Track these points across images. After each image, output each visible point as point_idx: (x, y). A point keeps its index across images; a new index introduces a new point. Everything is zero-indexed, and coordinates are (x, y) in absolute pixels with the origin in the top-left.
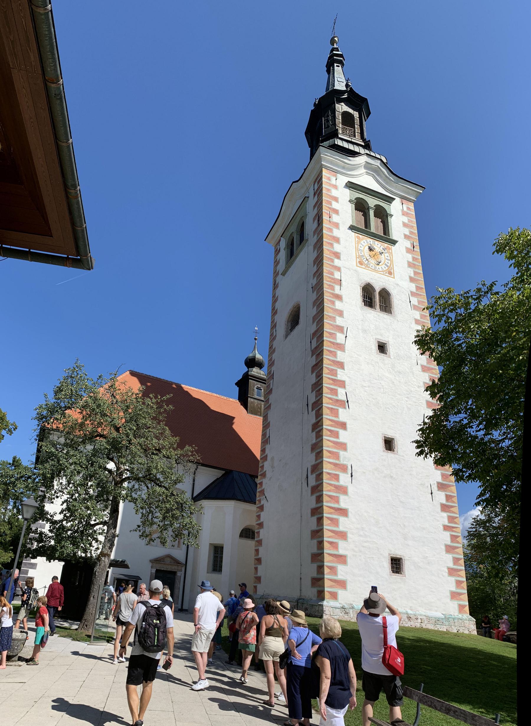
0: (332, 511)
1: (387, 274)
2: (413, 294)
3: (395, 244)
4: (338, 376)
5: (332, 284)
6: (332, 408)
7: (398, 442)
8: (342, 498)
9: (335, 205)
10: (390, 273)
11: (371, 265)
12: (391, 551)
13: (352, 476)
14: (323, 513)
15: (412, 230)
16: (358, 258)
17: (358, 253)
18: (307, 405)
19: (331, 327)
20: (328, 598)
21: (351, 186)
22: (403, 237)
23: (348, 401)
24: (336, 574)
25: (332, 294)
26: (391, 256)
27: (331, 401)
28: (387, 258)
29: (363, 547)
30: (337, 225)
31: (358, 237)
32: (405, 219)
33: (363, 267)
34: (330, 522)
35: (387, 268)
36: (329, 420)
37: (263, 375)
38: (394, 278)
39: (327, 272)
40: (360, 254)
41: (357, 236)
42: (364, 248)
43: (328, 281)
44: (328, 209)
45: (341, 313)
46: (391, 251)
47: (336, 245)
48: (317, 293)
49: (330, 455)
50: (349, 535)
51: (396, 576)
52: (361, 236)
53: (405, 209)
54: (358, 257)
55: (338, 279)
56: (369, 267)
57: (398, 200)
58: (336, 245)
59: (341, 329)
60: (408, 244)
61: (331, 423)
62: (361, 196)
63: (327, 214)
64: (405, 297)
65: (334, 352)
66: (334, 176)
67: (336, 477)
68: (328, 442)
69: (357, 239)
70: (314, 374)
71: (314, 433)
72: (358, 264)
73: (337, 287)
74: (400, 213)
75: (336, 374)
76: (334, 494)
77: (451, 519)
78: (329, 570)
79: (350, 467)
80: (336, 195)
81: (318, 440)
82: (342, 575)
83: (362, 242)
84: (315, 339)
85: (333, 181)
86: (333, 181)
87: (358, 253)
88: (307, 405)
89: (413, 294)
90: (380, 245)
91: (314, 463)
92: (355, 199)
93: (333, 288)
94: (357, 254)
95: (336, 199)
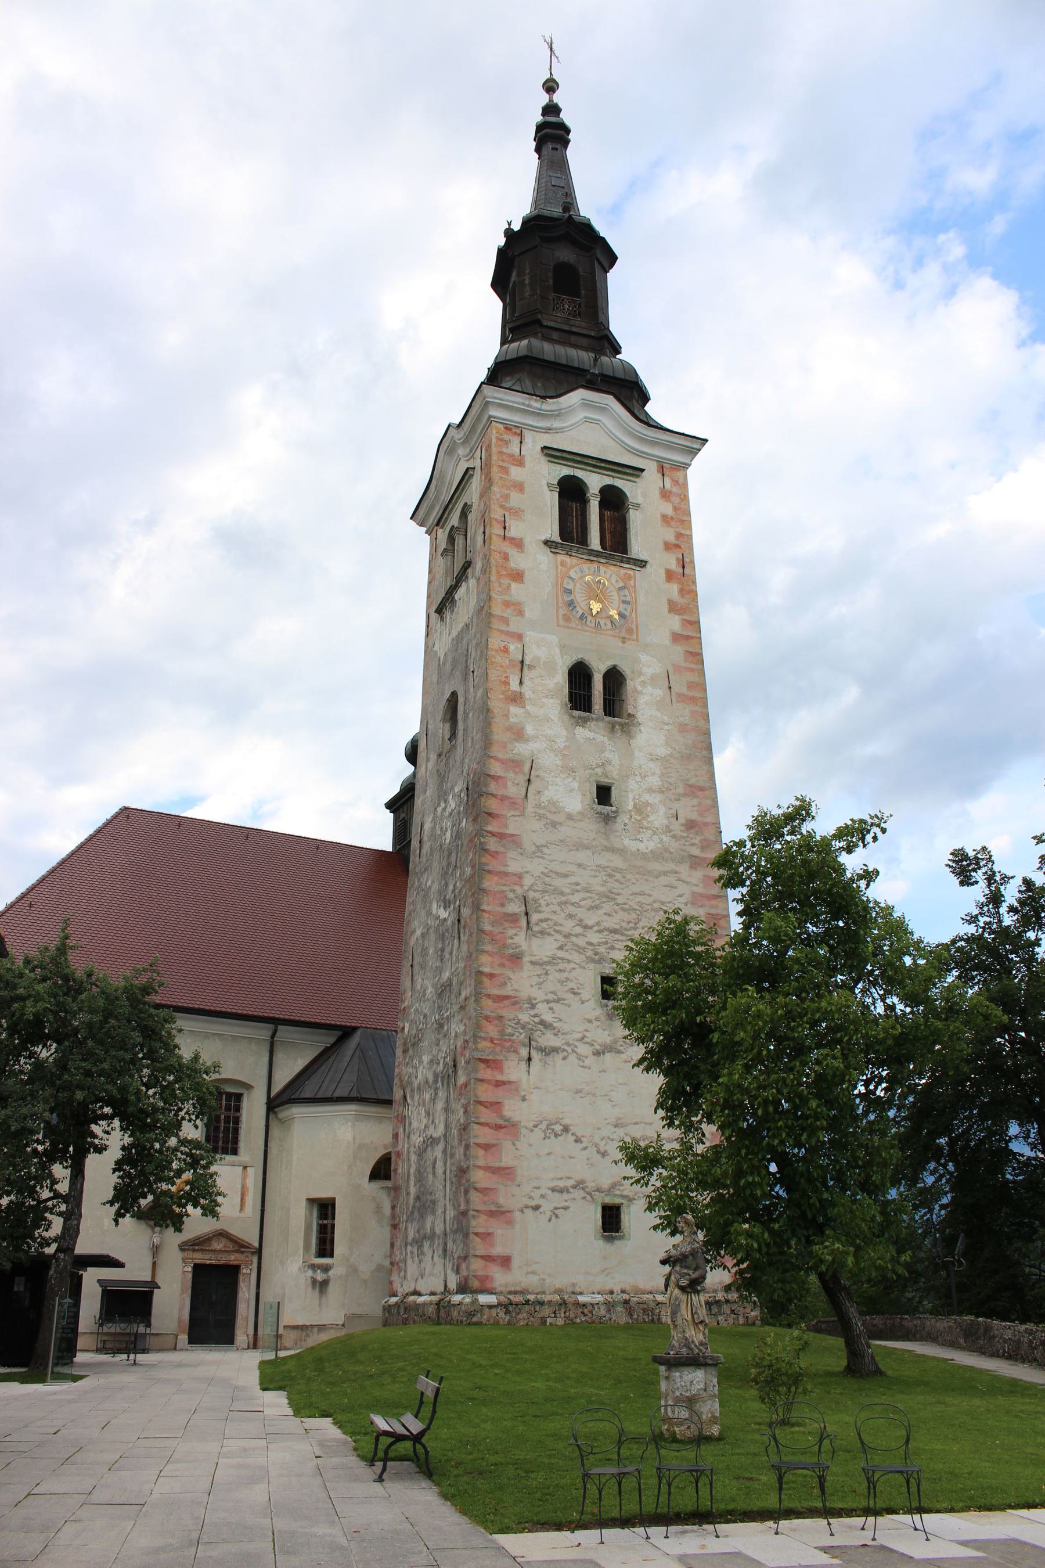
3: (645, 566)
9: (515, 499)
21: (552, 454)
28: (624, 599)
30: (518, 544)
31: (563, 564)
33: (573, 625)
42: (575, 586)
46: (632, 583)
57: (651, 468)
69: (560, 567)
72: (561, 622)
74: (656, 494)
80: (519, 479)
95: (520, 487)
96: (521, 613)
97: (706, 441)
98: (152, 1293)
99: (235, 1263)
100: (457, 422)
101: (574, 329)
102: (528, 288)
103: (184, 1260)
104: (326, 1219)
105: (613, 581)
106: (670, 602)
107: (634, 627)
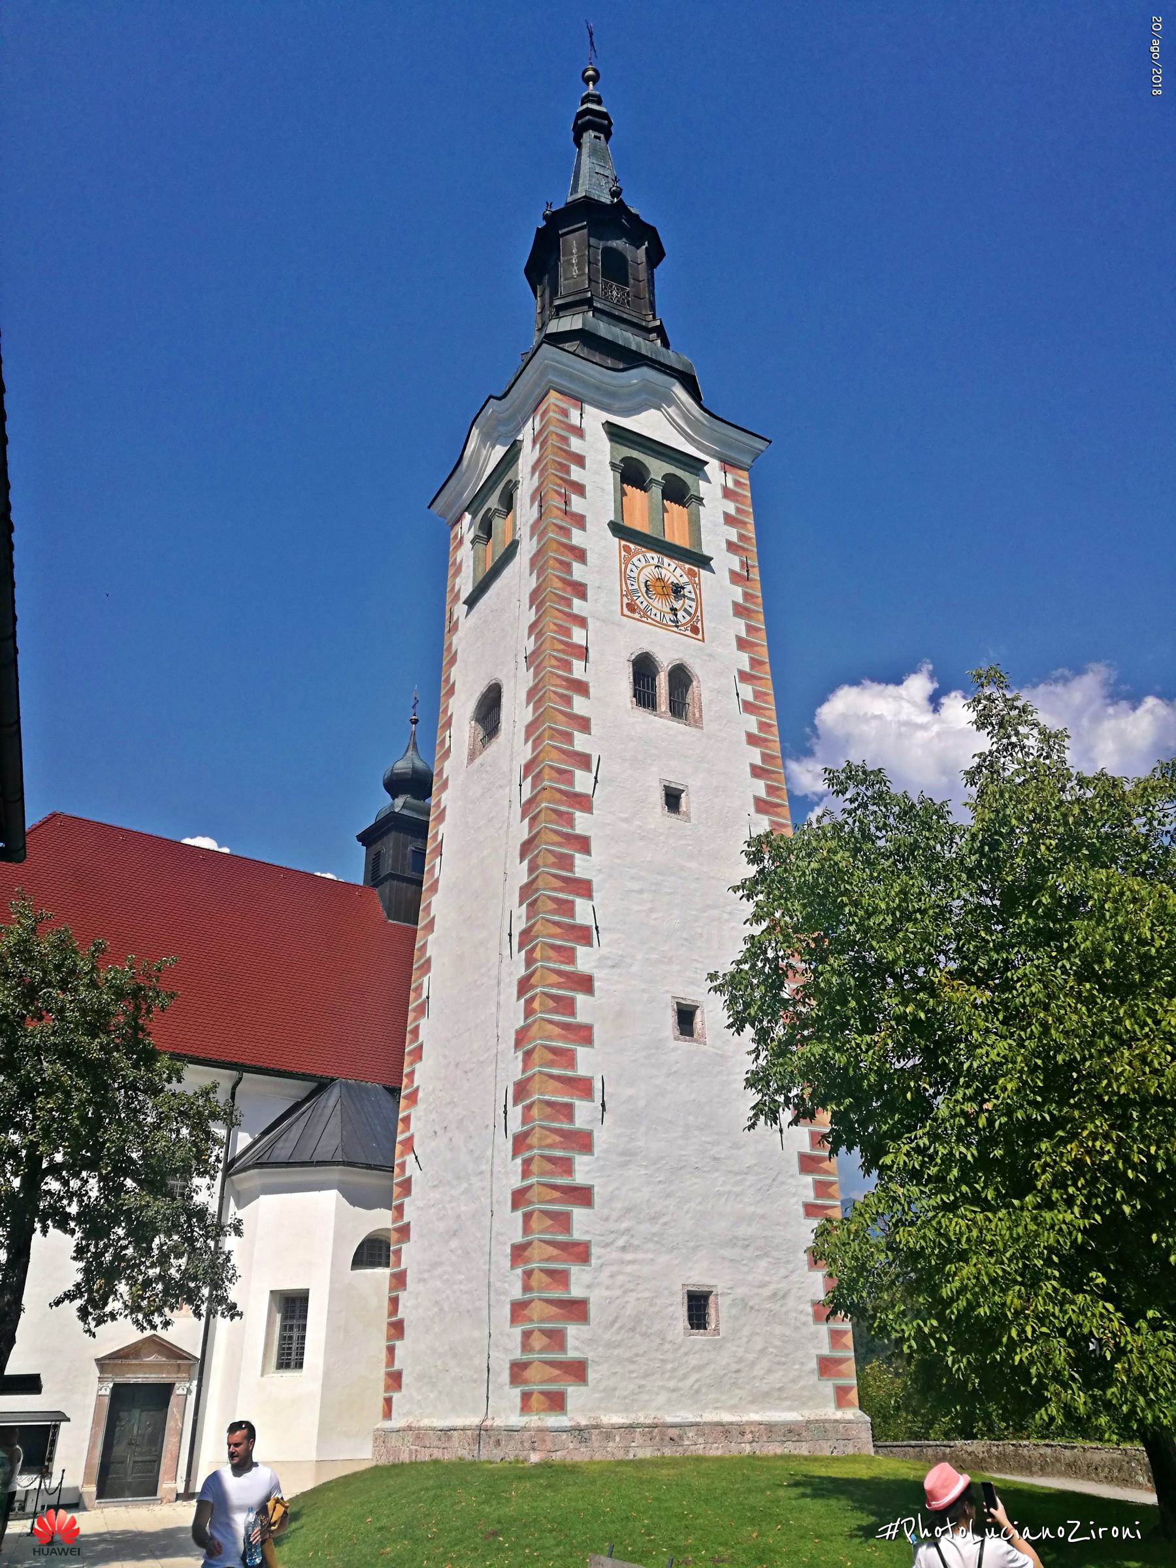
0: (556, 1194)
1: (688, 633)
2: (744, 677)
4: (577, 869)
5: (566, 657)
8: (581, 1162)
10: (695, 630)
11: (654, 611)
13: (603, 1105)
15: (743, 532)
16: (626, 595)
17: (626, 583)
18: (510, 935)
19: (563, 756)
20: (544, 1410)
22: (724, 546)
23: (597, 928)
24: (562, 1347)
25: (567, 680)
26: (698, 591)
31: (627, 549)
32: (730, 507)
33: (637, 616)
34: (550, 1222)
35: (688, 618)
38: (703, 640)
39: (555, 628)
40: (630, 588)
41: (624, 546)
43: (558, 651)
44: (559, 481)
45: (584, 724)
47: (576, 566)
48: (535, 675)
50: (595, 1251)
51: (699, 1337)
52: (632, 546)
53: (730, 485)
54: (624, 593)
55: (580, 647)
56: (648, 617)
57: (713, 467)
58: (576, 566)
59: (584, 761)
60: (735, 563)
61: (555, 979)
62: (635, 454)
63: (559, 493)
65: (568, 813)
66: (575, 407)
69: (623, 553)
70: (526, 862)
72: (626, 611)
73: (578, 665)
74: (719, 493)
75: (570, 866)
77: (821, 1188)
78: (546, 1340)
81: (530, 1020)
82: (576, 1349)
83: (635, 560)
84: (529, 779)
85: (574, 417)
86: (574, 417)
87: (626, 583)
88: (510, 935)
89: (744, 677)
90: (673, 566)
91: (520, 1077)
92: (622, 461)
93: (568, 666)
94: (624, 588)
96: (583, 596)
97: (770, 442)
98: (57, 1427)
99: (167, 1381)
100: (499, 395)
101: (625, 316)
102: (576, 268)
103: (101, 1380)
104: (292, 1318)
105: (678, 576)
106: (735, 604)
107: (699, 625)
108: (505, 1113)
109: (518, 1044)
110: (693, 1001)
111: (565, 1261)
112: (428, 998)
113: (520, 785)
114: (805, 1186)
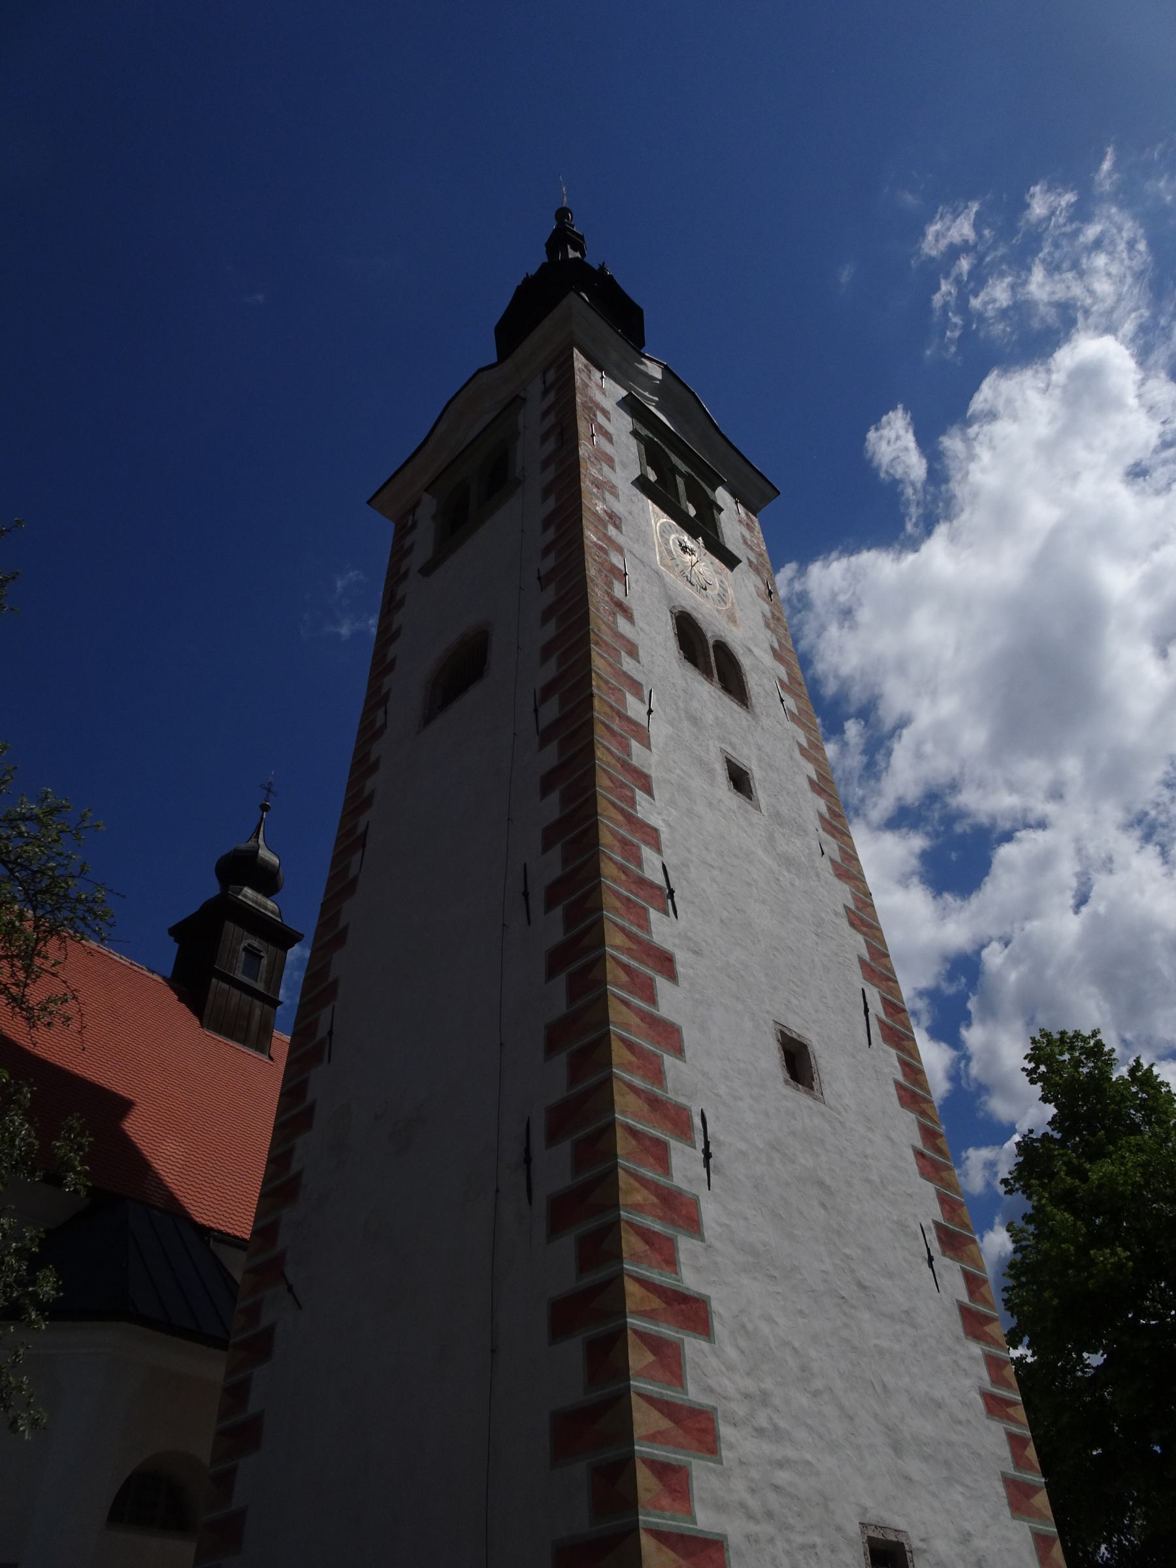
6: (628, 899)
7: (820, 1061)
12: (865, 1510)
14: (623, 1315)
18: (526, 894)
23: (672, 892)
27: (623, 877)
29: (776, 1488)
36: (623, 930)
37: (273, 912)
49: (633, 1059)
64: (771, 685)
67: (660, 1154)
68: (624, 1009)
71: (561, 980)
76: (657, 1227)
79: (697, 1121)
88: (526, 894)
108: (528, 1160)
109: (552, 1045)
110: (799, 1036)
111: (680, 1446)
112: (330, 1033)
113: (536, 711)
114: (972, 1358)
